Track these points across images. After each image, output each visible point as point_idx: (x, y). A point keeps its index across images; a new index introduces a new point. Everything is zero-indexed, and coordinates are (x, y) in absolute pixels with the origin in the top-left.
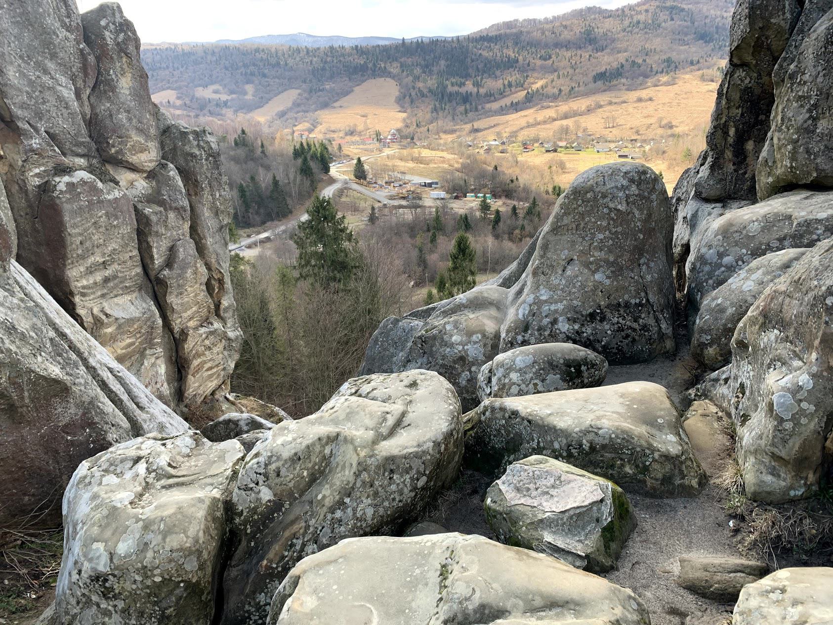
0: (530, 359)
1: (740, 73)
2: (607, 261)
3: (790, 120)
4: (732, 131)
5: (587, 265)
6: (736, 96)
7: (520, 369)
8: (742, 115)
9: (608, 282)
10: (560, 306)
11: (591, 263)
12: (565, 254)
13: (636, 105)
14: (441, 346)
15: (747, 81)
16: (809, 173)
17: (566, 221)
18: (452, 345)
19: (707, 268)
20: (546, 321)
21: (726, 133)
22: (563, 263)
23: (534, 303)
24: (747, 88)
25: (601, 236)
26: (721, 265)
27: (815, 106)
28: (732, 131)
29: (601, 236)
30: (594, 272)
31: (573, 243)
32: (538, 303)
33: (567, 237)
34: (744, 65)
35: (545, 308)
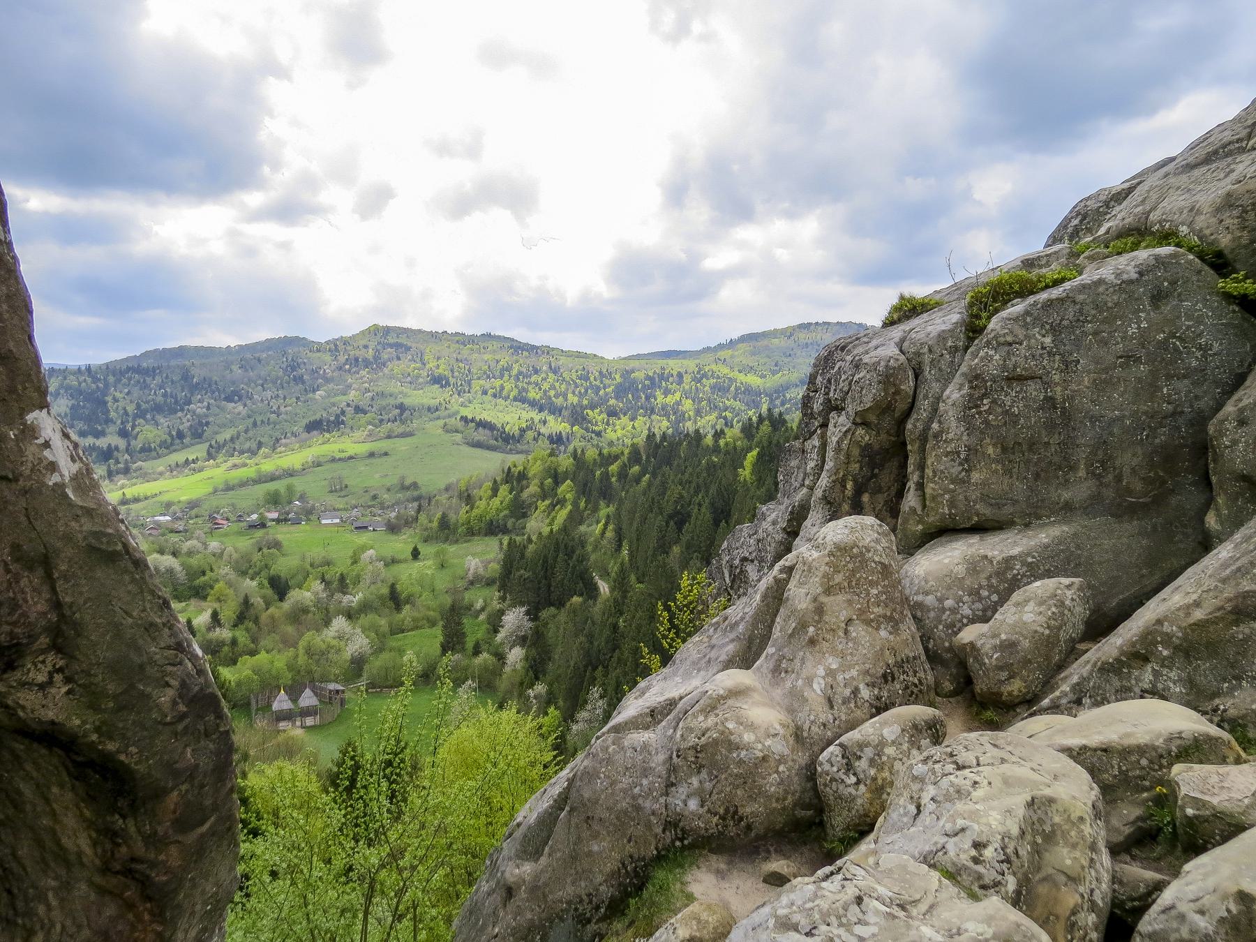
0: (896, 729)
1: (860, 431)
2: (885, 616)
3: (942, 472)
4: (849, 485)
5: (868, 622)
6: (856, 452)
7: (893, 742)
8: (861, 468)
9: (892, 637)
10: (854, 673)
11: (872, 621)
12: (843, 615)
13: (368, 461)
14: (730, 751)
15: (867, 438)
16: (969, 519)
17: (839, 578)
18: (748, 747)
19: (932, 614)
20: (847, 692)
21: (845, 487)
22: (843, 625)
23: (827, 675)
24: (867, 445)
25: (875, 591)
26: (943, 610)
27: (966, 460)
28: (849, 485)
29: (875, 591)
30: (878, 629)
31: (850, 602)
32: (831, 673)
33: (841, 598)
34: (865, 424)
35: (840, 677)
